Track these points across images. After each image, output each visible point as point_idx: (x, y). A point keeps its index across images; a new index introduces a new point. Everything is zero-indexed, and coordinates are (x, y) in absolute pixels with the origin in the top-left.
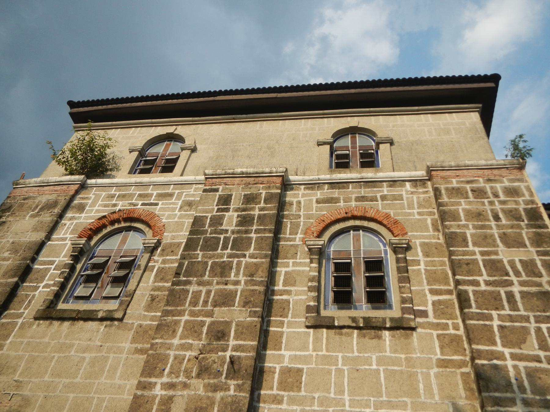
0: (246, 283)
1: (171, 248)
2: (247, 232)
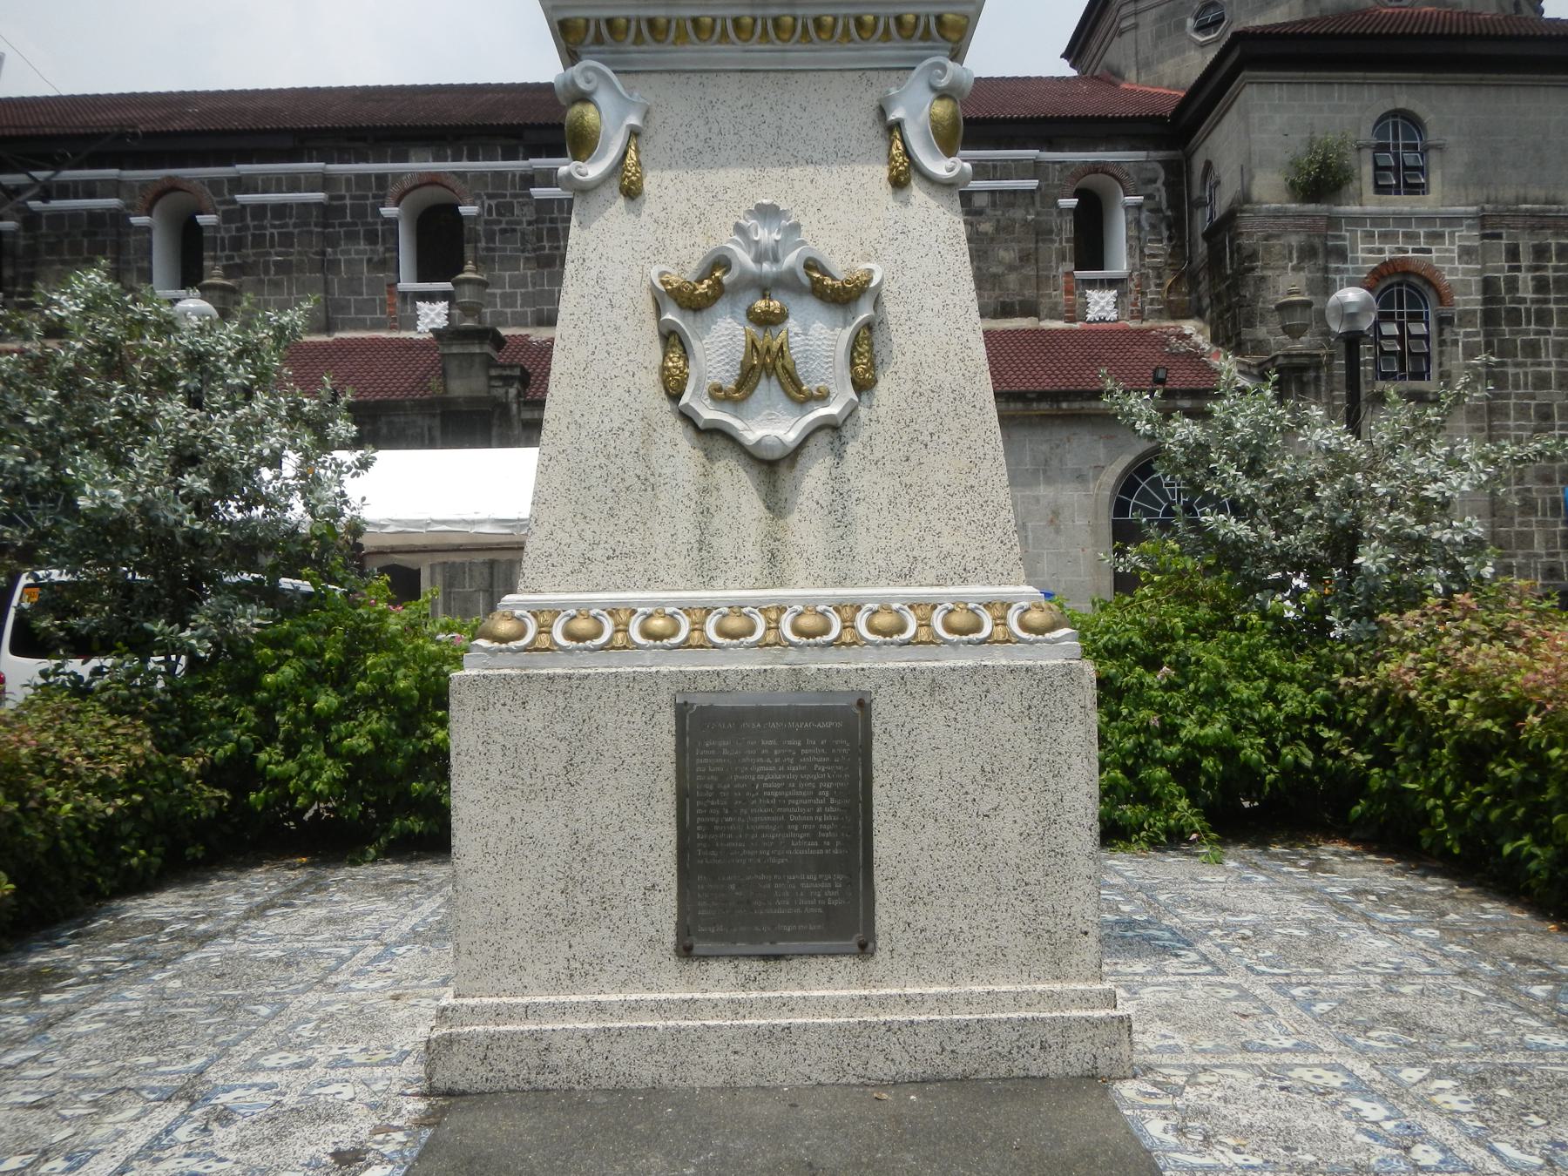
0: (1559, 364)
1: (1466, 317)
2: (1547, 301)
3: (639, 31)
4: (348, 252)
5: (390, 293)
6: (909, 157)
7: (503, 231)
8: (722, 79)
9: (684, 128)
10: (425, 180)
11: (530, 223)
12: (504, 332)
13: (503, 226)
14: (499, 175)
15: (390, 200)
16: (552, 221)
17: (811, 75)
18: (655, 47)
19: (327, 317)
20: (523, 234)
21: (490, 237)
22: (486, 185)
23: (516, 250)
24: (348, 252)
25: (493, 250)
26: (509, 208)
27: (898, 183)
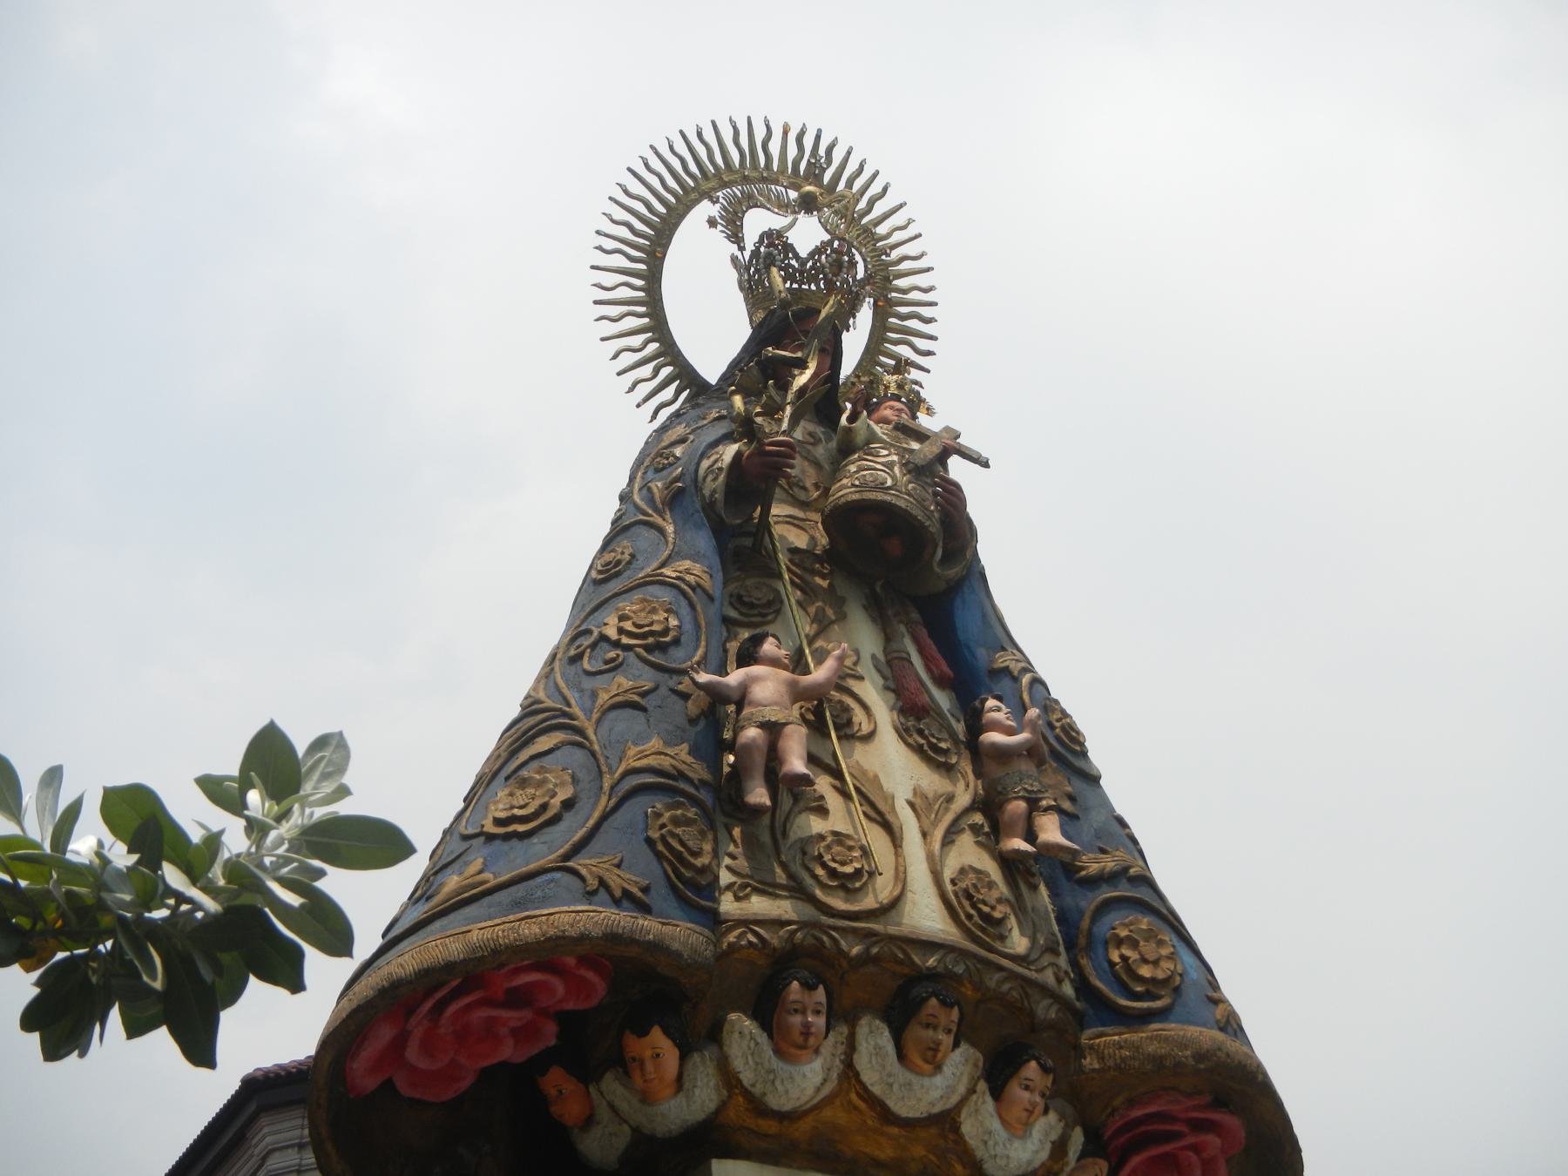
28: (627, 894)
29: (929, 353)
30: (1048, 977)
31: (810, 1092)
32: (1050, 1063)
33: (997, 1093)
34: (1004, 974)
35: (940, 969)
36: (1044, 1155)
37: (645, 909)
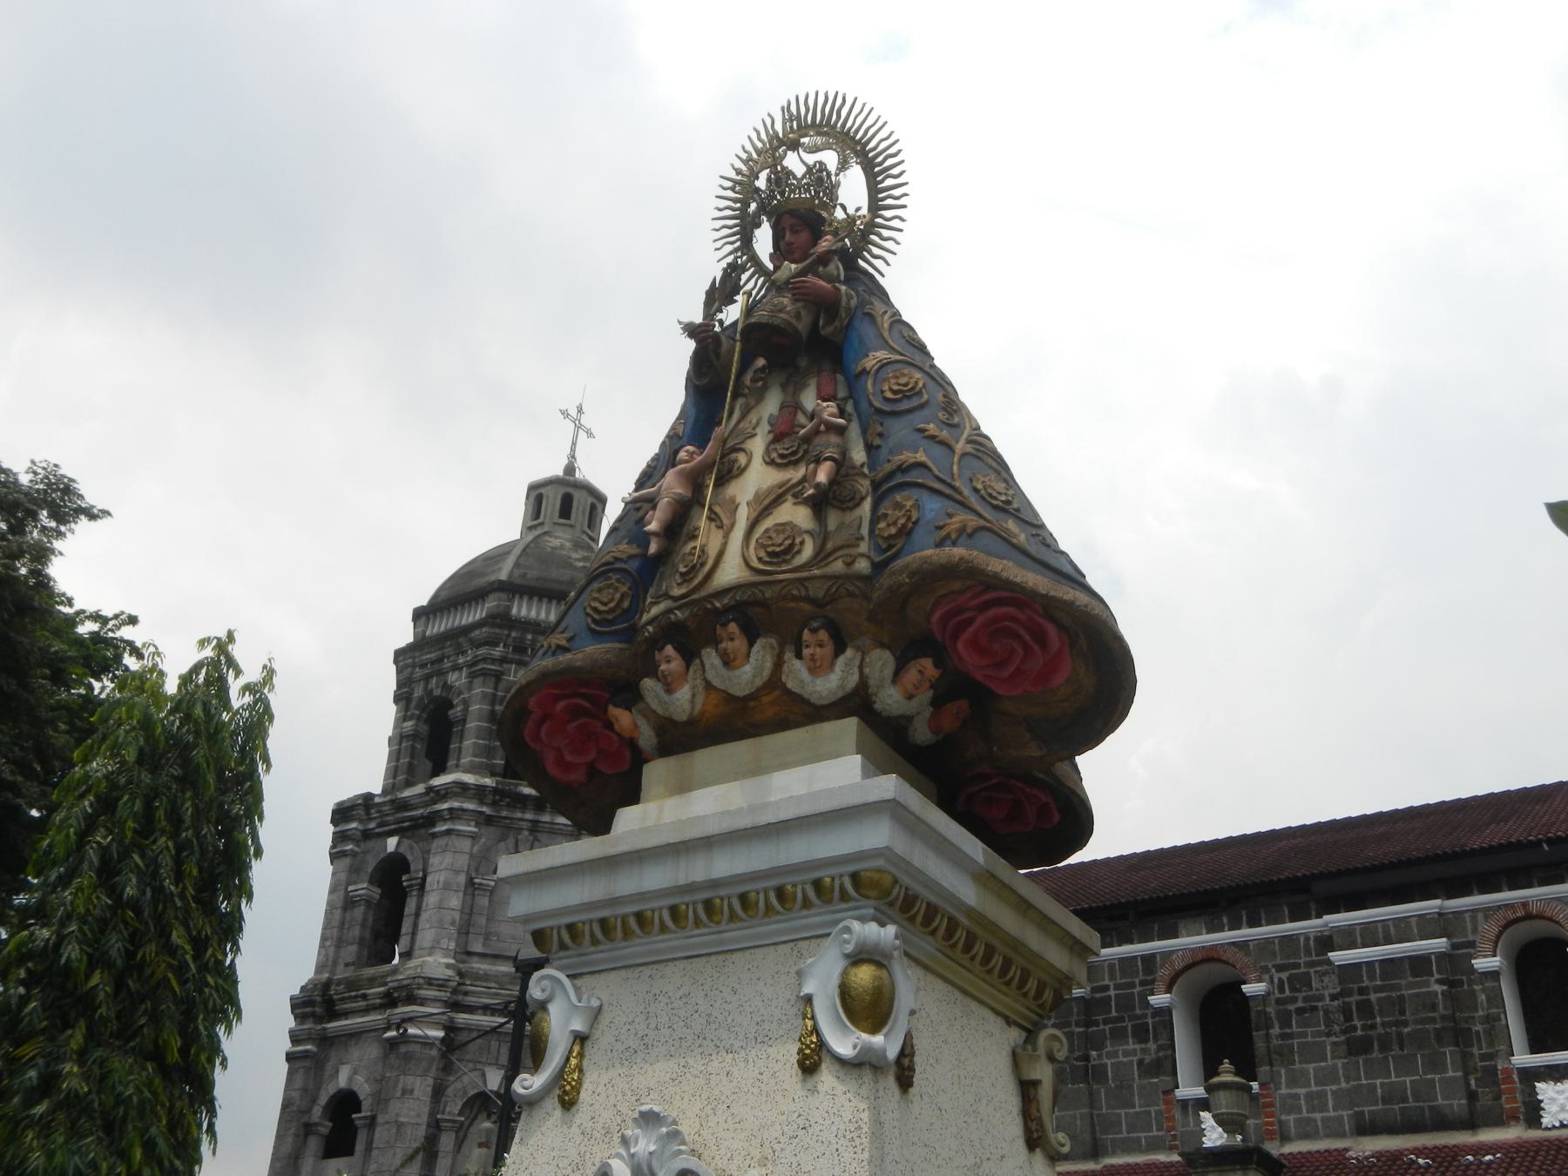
3: (592, 935)
4: (1114, 1054)
5: (1167, 1103)
6: (818, 1035)
7: (1301, 1011)
8: (669, 969)
9: (628, 1026)
10: (1199, 957)
11: (1333, 997)
12: (1274, 1149)
13: (1300, 1004)
14: (1289, 941)
15: (1160, 985)
16: (1362, 991)
17: (747, 953)
18: (609, 946)
19: (1095, 1140)
20: (1326, 1012)
21: (1285, 1020)
22: (1274, 954)
23: (1319, 1034)
24: (1114, 1054)
25: (1291, 1036)
26: (1305, 981)
27: (809, 1066)
28: (559, 647)
29: (902, 173)
30: (838, 566)
31: (687, 706)
32: (815, 625)
33: (799, 656)
34: (784, 584)
35: (733, 603)
36: (854, 679)
37: (566, 650)
